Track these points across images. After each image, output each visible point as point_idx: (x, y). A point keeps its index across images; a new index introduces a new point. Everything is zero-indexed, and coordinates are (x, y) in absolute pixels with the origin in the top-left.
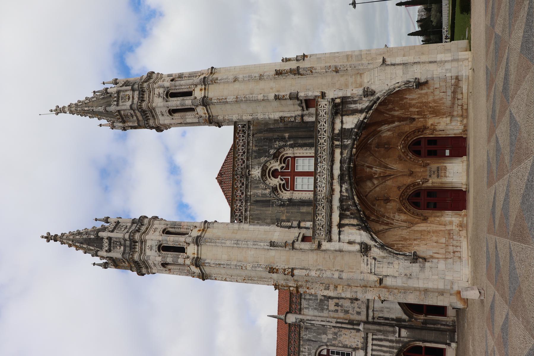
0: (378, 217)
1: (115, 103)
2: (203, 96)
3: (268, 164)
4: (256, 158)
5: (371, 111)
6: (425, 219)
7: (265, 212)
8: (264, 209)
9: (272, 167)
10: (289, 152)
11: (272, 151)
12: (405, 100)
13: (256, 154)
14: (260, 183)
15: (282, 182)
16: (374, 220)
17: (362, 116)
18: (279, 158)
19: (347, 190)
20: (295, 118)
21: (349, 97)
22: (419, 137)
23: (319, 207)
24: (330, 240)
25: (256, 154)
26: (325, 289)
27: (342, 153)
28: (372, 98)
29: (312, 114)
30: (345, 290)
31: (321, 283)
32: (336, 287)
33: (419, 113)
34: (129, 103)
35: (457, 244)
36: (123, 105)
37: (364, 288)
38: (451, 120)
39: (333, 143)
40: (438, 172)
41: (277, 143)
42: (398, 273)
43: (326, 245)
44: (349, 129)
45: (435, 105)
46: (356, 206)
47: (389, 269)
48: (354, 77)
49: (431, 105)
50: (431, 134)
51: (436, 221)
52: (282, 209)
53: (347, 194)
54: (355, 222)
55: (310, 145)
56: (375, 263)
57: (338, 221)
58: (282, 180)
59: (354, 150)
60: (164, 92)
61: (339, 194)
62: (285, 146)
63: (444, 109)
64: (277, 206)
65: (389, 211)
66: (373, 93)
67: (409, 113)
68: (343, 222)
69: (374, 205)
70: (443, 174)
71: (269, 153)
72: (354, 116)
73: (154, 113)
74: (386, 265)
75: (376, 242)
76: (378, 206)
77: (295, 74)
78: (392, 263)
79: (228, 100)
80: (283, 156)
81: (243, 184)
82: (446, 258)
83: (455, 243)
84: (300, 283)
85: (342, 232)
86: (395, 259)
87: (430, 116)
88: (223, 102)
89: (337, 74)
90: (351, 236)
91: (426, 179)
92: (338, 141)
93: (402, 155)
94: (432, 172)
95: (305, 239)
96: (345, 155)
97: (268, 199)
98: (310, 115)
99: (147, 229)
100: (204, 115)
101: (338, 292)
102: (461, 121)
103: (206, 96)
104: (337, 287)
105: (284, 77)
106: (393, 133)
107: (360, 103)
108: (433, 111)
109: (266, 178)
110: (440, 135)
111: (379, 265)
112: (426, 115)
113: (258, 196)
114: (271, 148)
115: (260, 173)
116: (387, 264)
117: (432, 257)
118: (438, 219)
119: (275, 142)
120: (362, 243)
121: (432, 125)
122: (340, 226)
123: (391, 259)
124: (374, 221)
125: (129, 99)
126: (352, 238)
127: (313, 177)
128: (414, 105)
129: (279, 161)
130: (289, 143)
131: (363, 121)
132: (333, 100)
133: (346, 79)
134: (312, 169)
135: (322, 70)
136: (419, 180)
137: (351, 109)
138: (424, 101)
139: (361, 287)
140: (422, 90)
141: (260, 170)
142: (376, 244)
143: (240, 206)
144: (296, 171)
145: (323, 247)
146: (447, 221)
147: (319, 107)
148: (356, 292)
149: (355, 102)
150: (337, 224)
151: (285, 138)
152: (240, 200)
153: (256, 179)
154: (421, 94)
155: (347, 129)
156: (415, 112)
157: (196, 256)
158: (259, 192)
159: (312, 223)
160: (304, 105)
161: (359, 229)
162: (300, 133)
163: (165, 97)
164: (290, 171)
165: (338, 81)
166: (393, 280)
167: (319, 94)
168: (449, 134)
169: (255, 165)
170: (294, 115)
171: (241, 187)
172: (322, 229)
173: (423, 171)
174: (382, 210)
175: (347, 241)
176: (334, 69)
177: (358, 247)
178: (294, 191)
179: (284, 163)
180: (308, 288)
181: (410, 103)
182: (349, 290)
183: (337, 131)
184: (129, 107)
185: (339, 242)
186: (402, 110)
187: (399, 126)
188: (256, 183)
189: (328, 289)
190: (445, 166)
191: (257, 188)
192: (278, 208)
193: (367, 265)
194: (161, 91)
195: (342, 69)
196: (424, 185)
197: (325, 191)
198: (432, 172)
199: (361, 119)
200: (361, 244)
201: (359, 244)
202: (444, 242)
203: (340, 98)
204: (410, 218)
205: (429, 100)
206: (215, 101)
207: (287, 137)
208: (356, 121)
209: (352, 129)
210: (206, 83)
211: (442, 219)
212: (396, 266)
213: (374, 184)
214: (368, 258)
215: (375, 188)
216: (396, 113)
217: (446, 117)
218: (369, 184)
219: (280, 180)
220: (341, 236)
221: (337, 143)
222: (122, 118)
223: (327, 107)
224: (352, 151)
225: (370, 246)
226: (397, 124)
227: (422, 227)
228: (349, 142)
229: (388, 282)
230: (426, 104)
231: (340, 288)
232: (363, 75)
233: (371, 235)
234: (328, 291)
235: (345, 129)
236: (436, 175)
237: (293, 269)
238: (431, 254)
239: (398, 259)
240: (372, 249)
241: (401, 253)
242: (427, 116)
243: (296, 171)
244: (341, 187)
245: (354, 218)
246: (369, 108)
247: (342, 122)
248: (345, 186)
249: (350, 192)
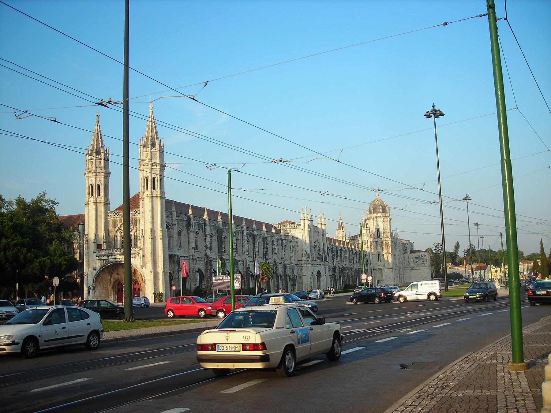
6: (113, 288)
43: (95, 254)
52: (113, 233)
54: (102, 265)
95: (99, 247)
99: (99, 176)
117: (95, 292)
122: (101, 259)
126: (97, 264)
130: (135, 233)
157: (89, 202)
158: (118, 223)
159: (105, 248)
166: (86, 280)
174: (114, 273)
177: (95, 267)
202: (103, 295)
204: (112, 283)
227: (110, 287)
233: (98, 271)
237: (88, 244)
238: (96, 291)
248: (113, 260)
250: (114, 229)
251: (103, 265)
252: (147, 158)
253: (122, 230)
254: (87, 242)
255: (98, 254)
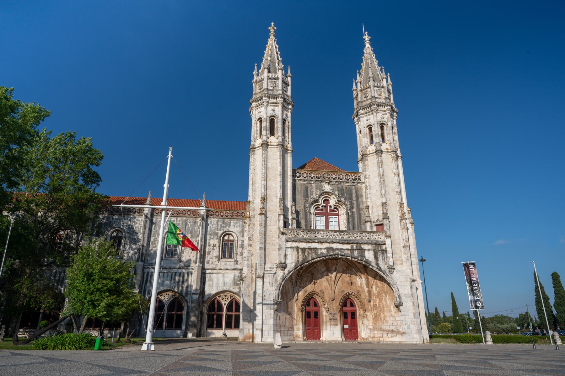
0: (301, 275)
1: (376, 85)
2: (383, 150)
3: (333, 196)
4: (338, 188)
5: (377, 271)
7: (300, 194)
8: (302, 194)
9: (331, 199)
10: (342, 211)
11: (343, 199)
12: (384, 295)
13: (340, 188)
14: (320, 191)
15: (320, 207)
16: (300, 273)
17: (374, 264)
18: (338, 205)
19: (322, 253)
20: (368, 216)
21: (386, 255)
22: (357, 306)
23: (309, 233)
24: (287, 241)
25: (340, 188)
26: (249, 237)
27: (347, 249)
28: (387, 271)
29: (372, 229)
30: (249, 252)
31: (253, 235)
32: (250, 245)
33: (375, 305)
34: (376, 96)
35: (285, 334)
36: (374, 90)
37: (251, 266)
38: (371, 329)
39: (354, 243)
40: (334, 319)
41: (349, 203)
42: (266, 290)
44: (364, 254)
45: (382, 318)
46: (312, 260)
47: (268, 284)
48: (400, 259)
49: (382, 314)
50: (359, 315)
51: (298, 318)
52: (303, 206)
53: (319, 253)
54: (301, 259)
55: (348, 227)
56: (272, 274)
57: (301, 247)
58: (322, 206)
59: (350, 259)
60: (385, 122)
61: (320, 248)
62: (347, 209)
63: (379, 323)
64: (305, 203)
65: (305, 284)
66: (391, 273)
67: (374, 298)
68: (300, 250)
69: (308, 273)
70: (332, 323)
71: (341, 197)
72: (374, 259)
73: (369, 114)
74: (271, 281)
75: (288, 274)
76: (308, 276)
77: (401, 217)
78: (272, 286)
79: (381, 169)
80: (340, 207)
81: (319, 178)
82: (277, 325)
83: (286, 332)
84: (252, 219)
85: (292, 249)
86: (276, 288)
87: (373, 314)
88: (380, 165)
89: (402, 247)
90: (291, 256)
91: (328, 310)
92: (356, 247)
93: (344, 293)
94: (333, 315)
96: (346, 252)
97: (309, 196)
98: (371, 227)
100: (368, 150)
101: (247, 247)
102: (370, 337)
103: (383, 153)
104: (251, 246)
105: (398, 209)
106: (359, 286)
107: (383, 263)
108: (377, 316)
109: (324, 195)
110: (359, 321)
111: (271, 276)
112: (374, 311)
113: (311, 189)
114: (346, 199)
115: (328, 191)
116: (272, 282)
118: (300, 320)
119: (350, 202)
120: (286, 264)
121: (367, 315)
122: (297, 248)
123: (276, 285)
124: (298, 272)
125: (379, 95)
126: (289, 257)
127: (325, 229)
128: (381, 302)
129: (336, 204)
130: (349, 211)
131: (371, 265)
132: (385, 244)
133: (398, 253)
134: (331, 228)
135: (404, 236)
136: (327, 306)
137: (379, 257)
138: (385, 309)
139: (251, 264)
140: (393, 307)
141: (329, 190)
142: (286, 274)
143: (303, 176)
144: (329, 216)
145: (282, 236)
146: (299, 326)
147: (379, 234)
148: (248, 260)
149: (383, 259)
150: (299, 246)
151: (352, 209)
152: (307, 176)
153: (322, 188)
154: (390, 307)
155: (364, 254)
156: (376, 303)
158: (314, 190)
160: (379, 223)
161: (295, 262)
162: (356, 220)
163: (381, 122)
164: (329, 212)
165: (397, 247)
167: (388, 234)
168: (359, 327)
169: (333, 187)
170: (370, 215)
171: (317, 177)
172: (294, 235)
173: (334, 308)
174: (305, 279)
175: (286, 254)
176: (406, 245)
177: (283, 261)
178: (315, 215)
179: (335, 208)
180: (249, 225)
181: (382, 299)
182: (249, 255)
183: (362, 246)
184: (373, 95)
185: (286, 248)
186: (377, 293)
187: (364, 291)
188: (319, 187)
189: (249, 240)
190: (338, 325)
191: (317, 189)
192: (303, 204)
193: (270, 268)
194: (386, 120)
195: (406, 250)
196: (324, 309)
197: (321, 237)
198: (333, 315)
199: (372, 264)
200: (285, 263)
201: (285, 262)
202: (286, 324)
203: (386, 249)
205: (386, 313)
206: (380, 160)
207: (353, 210)
208: (370, 260)
209: (365, 257)
210: (392, 153)
211: (301, 323)
212: (271, 289)
213: (323, 273)
214: (275, 269)
215: (320, 273)
216: (374, 289)
217: (372, 326)
218: (324, 269)
219: (322, 205)
220: (290, 249)
221: (355, 246)
222: (364, 90)
223: (379, 239)
224: (350, 257)
225: (284, 270)
226: (366, 289)
228: (355, 254)
229: (259, 282)
230: (382, 310)
231: (250, 248)
232: (402, 265)
233: (292, 271)
234: (248, 240)
235: (364, 252)
236: (332, 318)
239: (276, 290)
240: (282, 271)
241: (280, 292)
242: (372, 311)
243: (329, 216)
244: (325, 249)
245: (303, 258)
246: (380, 269)
247: (369, 250)
248: (324, 251)
249: (322, 255)
250: (305, 200)
251: (304, 259)
252: (381, 97)
253: (319, 203)
254: (264, 212)
255: (291, 236)
